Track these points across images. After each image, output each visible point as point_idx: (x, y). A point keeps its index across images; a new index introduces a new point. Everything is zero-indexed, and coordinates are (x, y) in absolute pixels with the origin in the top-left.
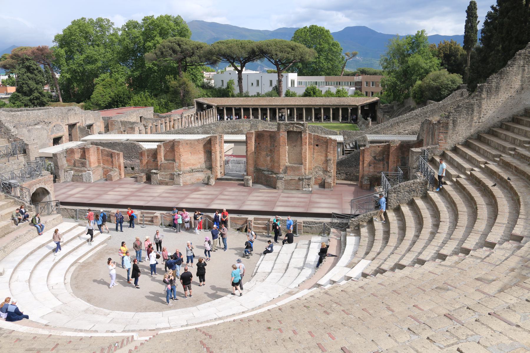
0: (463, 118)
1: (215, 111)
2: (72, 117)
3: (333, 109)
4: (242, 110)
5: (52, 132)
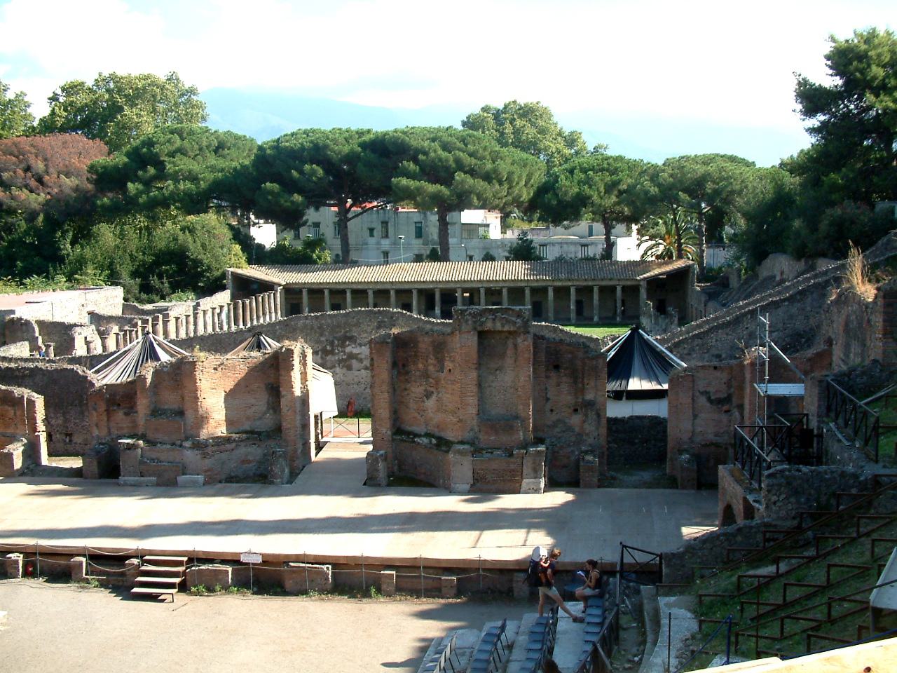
1: (278, 297)
4: (349, 295)
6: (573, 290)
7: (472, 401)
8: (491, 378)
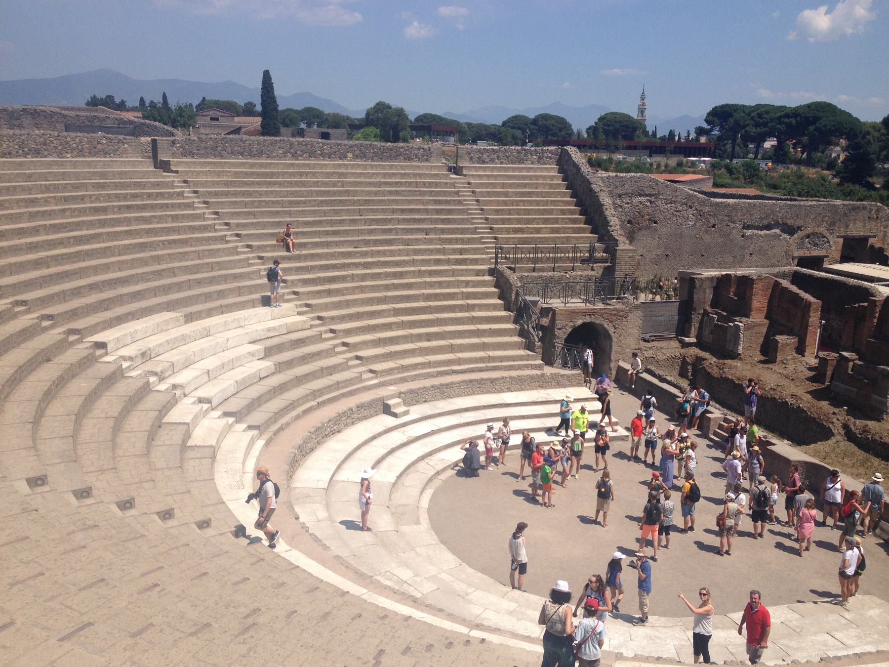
2: (859, 224)
5: (801, 246)
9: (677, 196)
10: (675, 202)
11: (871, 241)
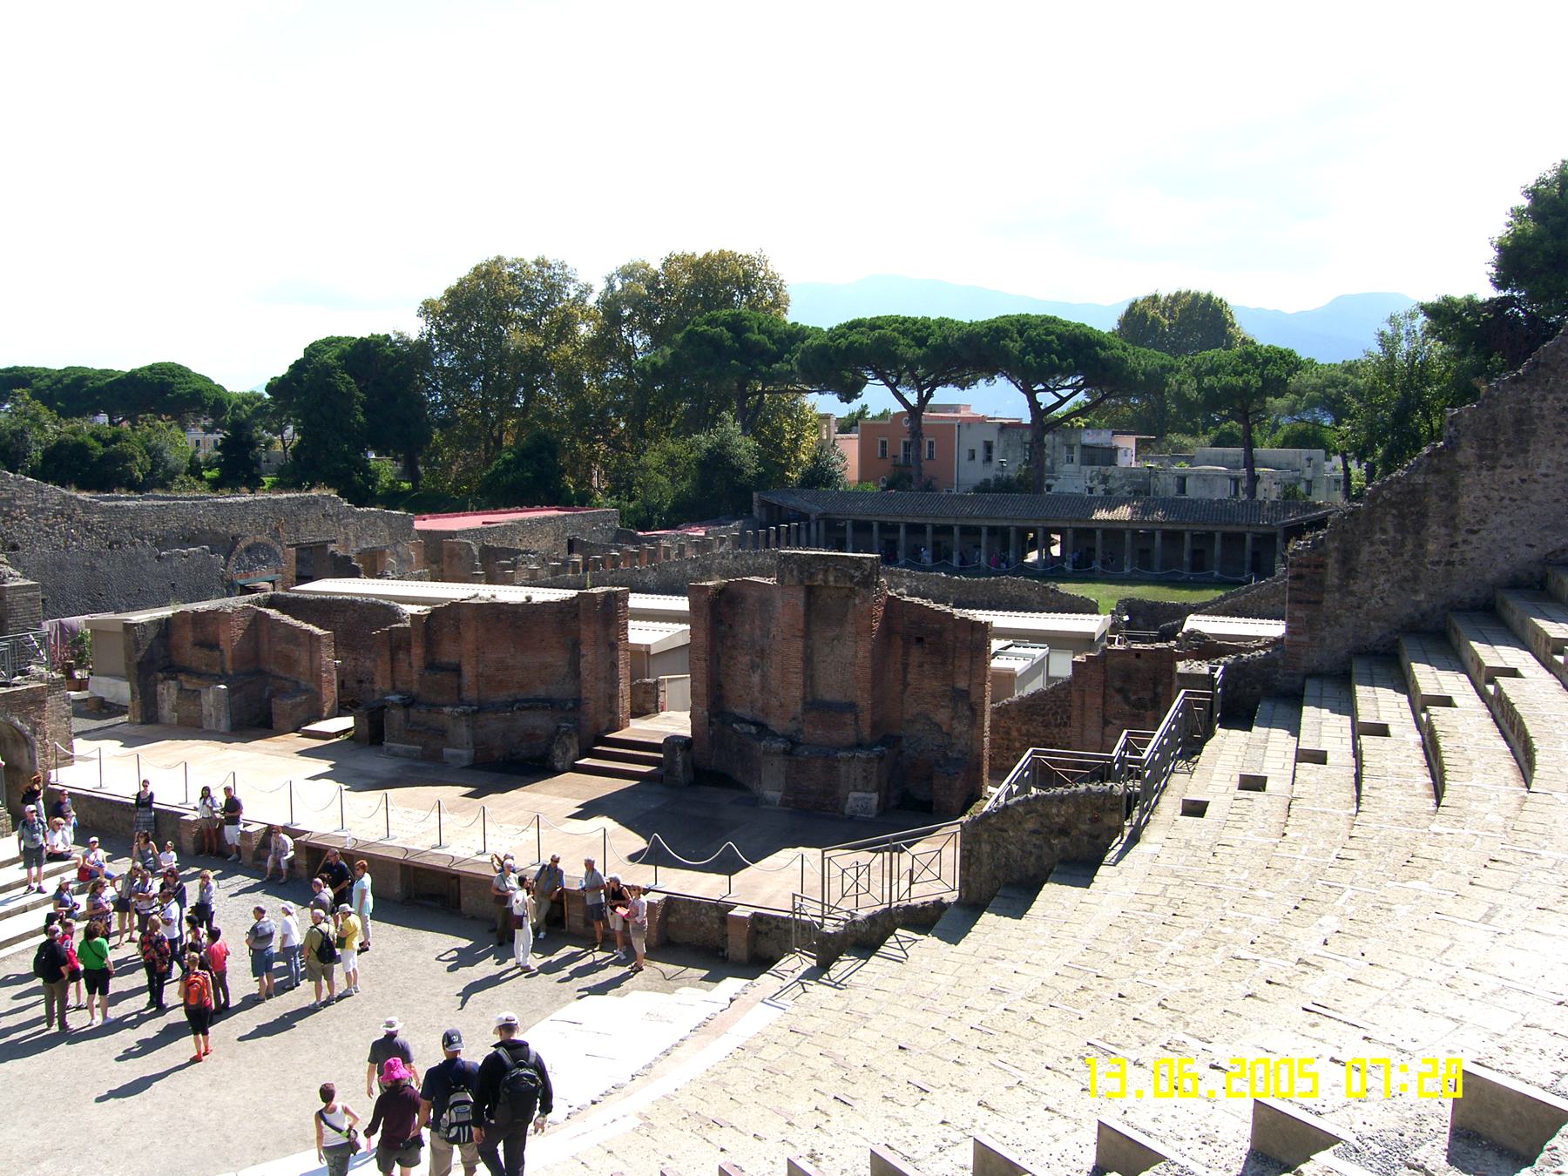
0: (1384, 543)
2: (312, 526)
3: (1193, 537)
4: (902, 530)
6: (1187, 536)
7: (797, 679)
8: (827, 650)
9: (44, 501)
10: (42, 510)
11: (332, 548)
